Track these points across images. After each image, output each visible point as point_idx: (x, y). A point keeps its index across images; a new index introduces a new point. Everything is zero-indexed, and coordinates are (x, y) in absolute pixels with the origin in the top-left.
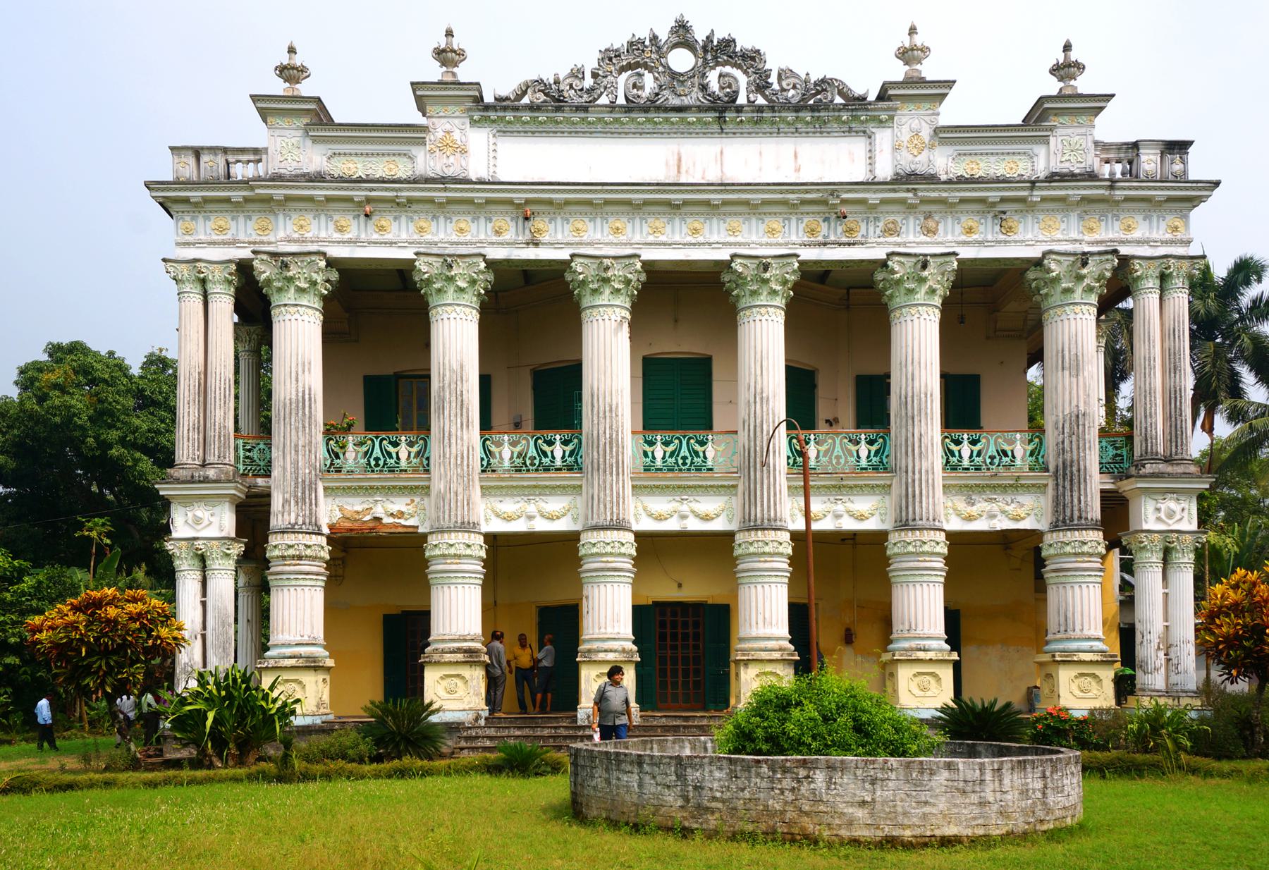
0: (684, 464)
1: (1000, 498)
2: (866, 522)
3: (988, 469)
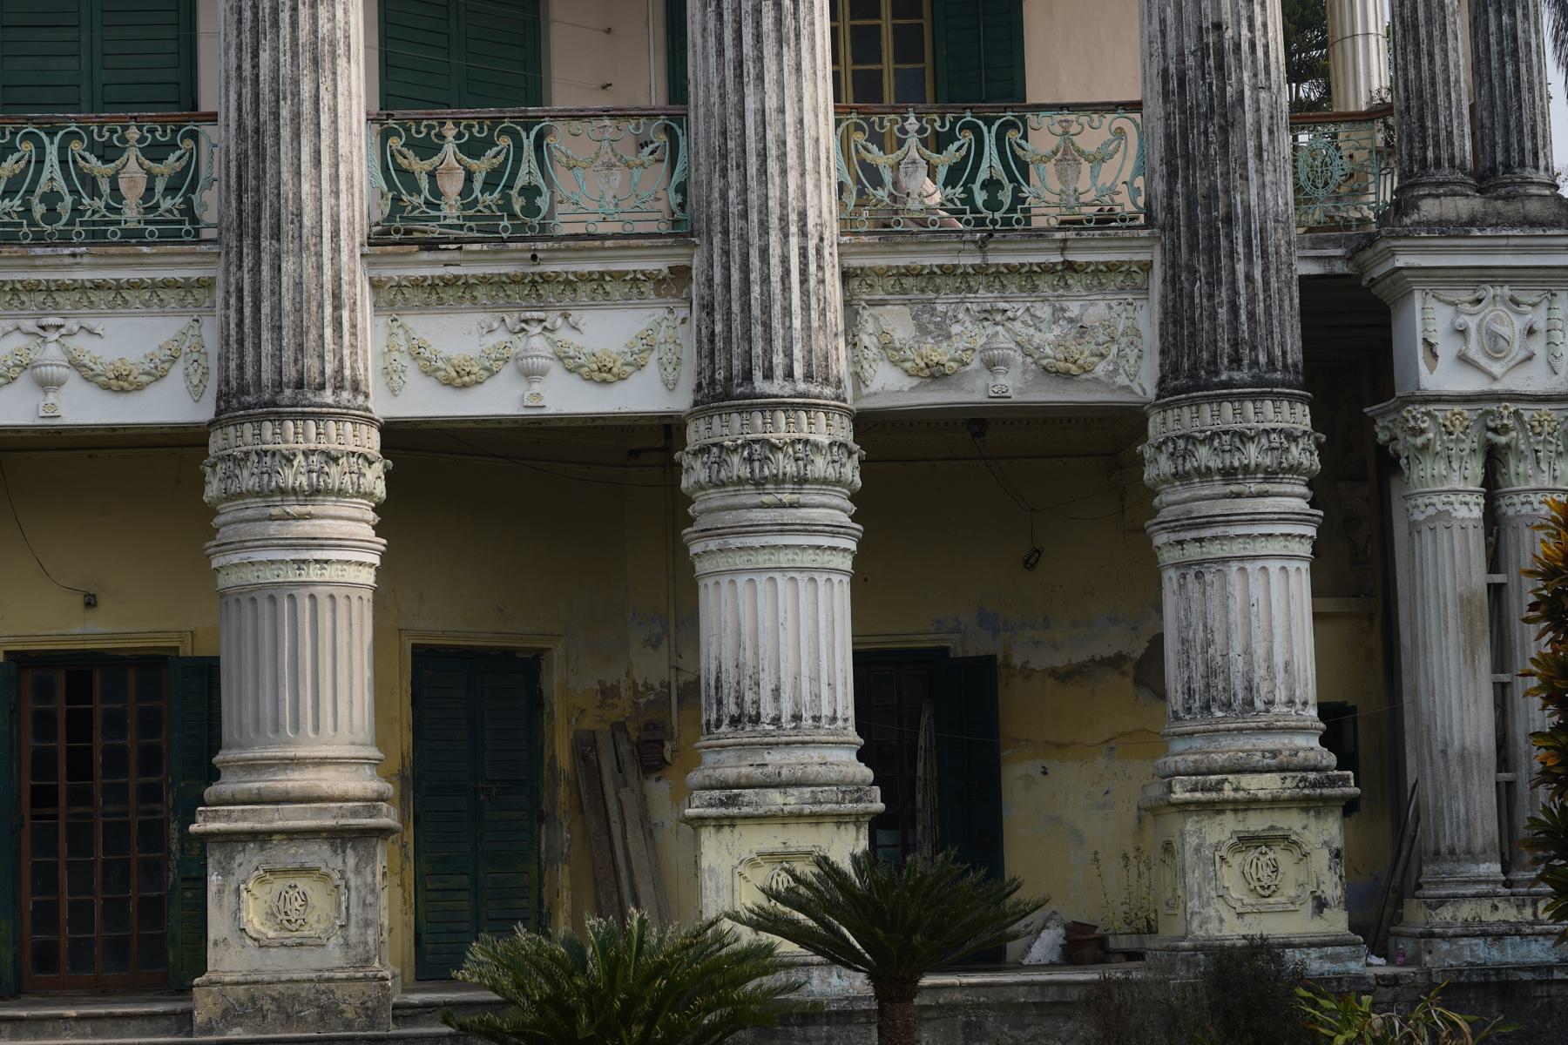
0: (52, 214)
1: (1018, 308)
2: (619, 387)
3: (981, 222)
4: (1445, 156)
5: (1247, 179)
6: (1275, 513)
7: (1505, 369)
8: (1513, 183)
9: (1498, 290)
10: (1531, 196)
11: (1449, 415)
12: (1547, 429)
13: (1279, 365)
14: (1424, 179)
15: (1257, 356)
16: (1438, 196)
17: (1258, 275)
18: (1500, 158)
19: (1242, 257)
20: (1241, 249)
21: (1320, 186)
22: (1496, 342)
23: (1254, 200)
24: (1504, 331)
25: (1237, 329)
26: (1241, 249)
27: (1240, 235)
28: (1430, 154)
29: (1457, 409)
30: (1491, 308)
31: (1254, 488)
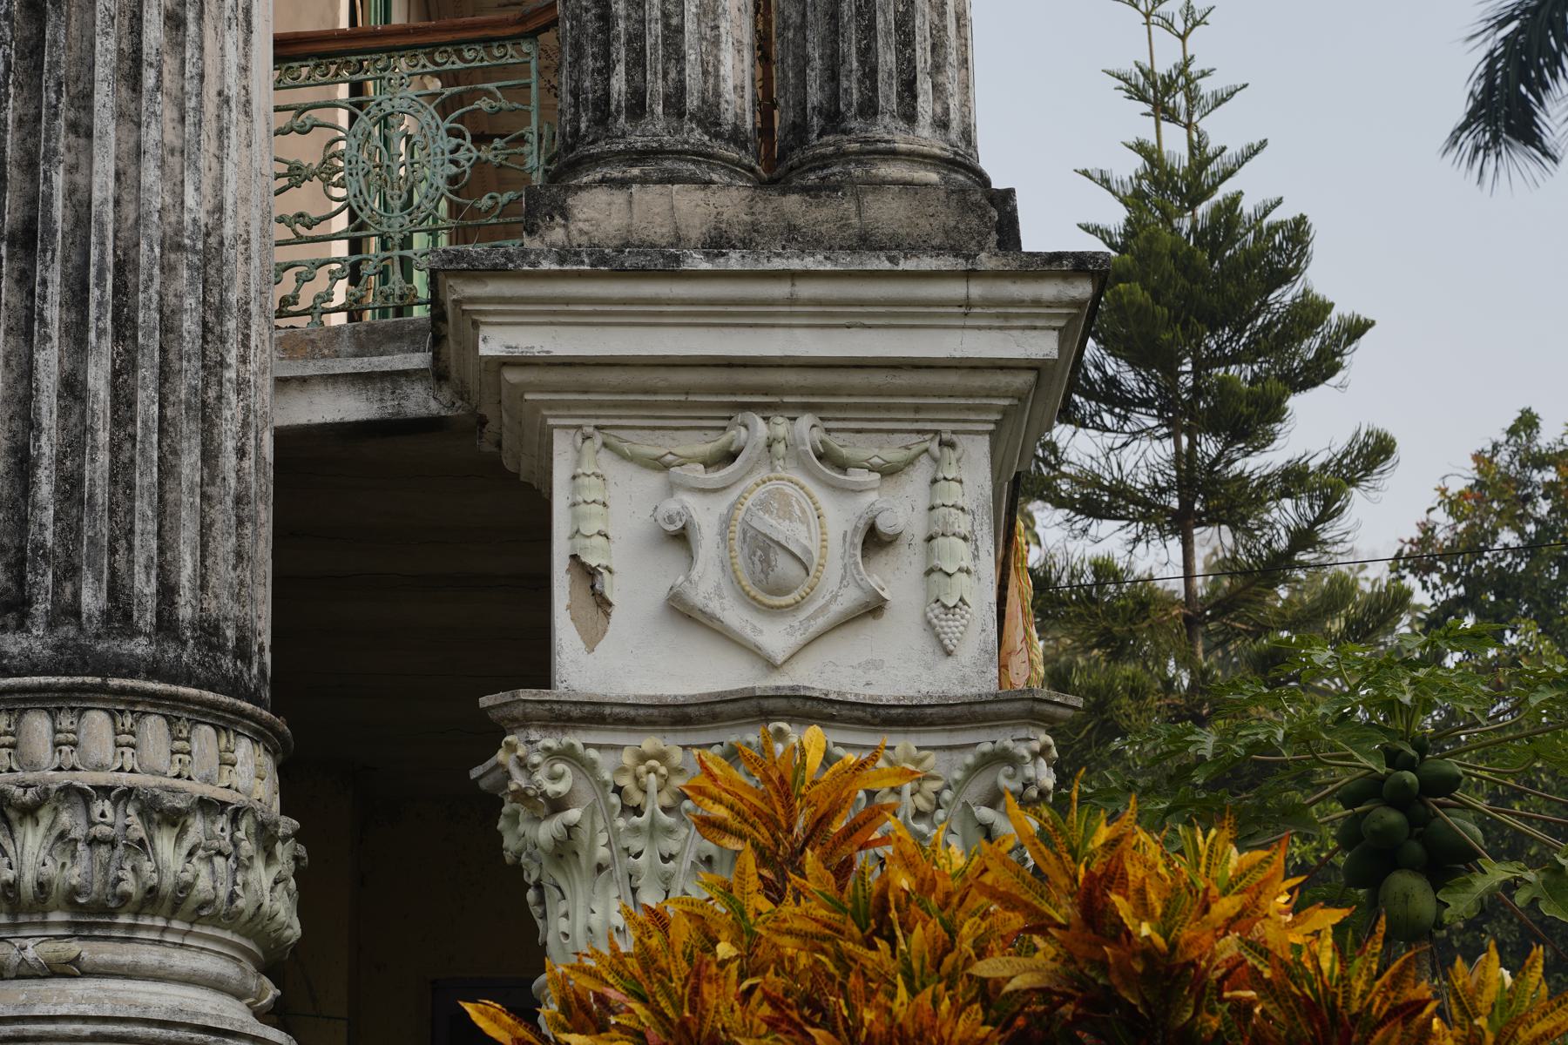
4: (657, 87)
5: (89, 135)
6: (85, 1019)
7: (799, 638)
8: (841, 155)
9: (781, 426)
10: (881, 184)
11: (627, 758)
12: (908, 803)
13: (146, 619)
14: (602, 147)
15: (76, 595)
16: (624, 184)
17: (98, 377)
18: (815, 96)
19: (54, 332)
20: (53, 313)
21: (396, 204)
22: (766, 562)
23: (103, 187)
24: (781, 529)
25: (25, 521)
26: (53, 313)
27: (55, 276)
28: (618, 83)
29: (650, 742)
30: (764, 473)
31: (34, 950)
